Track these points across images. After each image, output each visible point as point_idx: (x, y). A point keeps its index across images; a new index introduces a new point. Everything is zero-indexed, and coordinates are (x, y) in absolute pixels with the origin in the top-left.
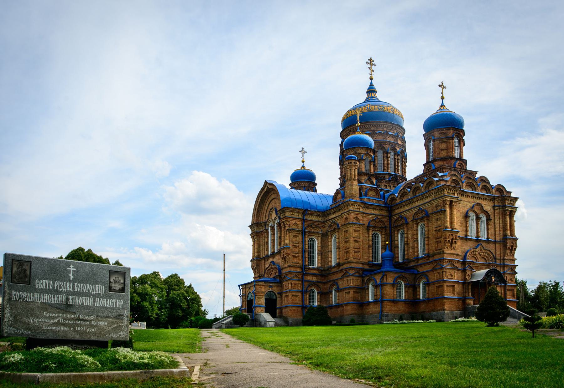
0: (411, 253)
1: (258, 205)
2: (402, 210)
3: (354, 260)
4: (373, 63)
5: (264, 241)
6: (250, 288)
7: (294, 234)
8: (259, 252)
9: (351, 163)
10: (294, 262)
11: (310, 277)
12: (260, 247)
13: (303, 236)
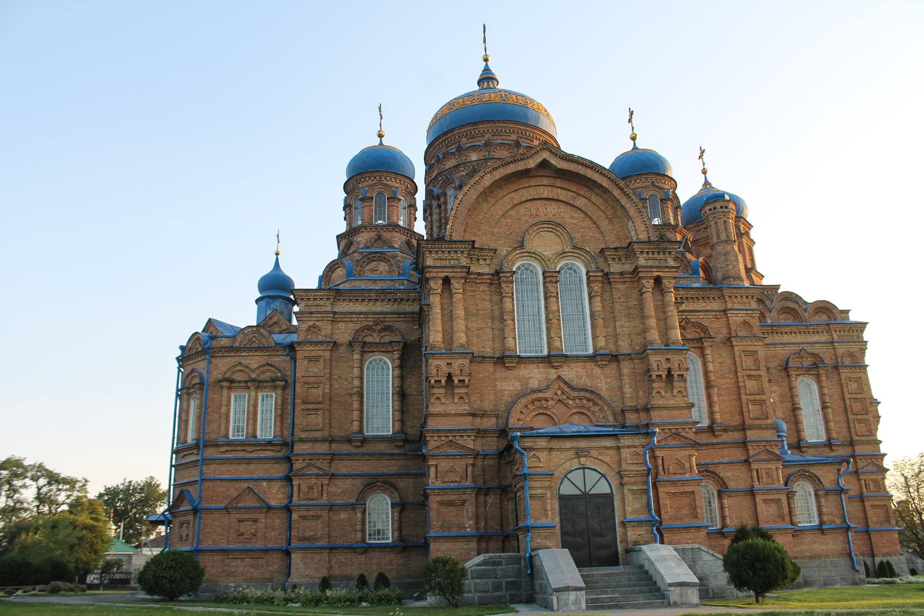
9: (726, 207)
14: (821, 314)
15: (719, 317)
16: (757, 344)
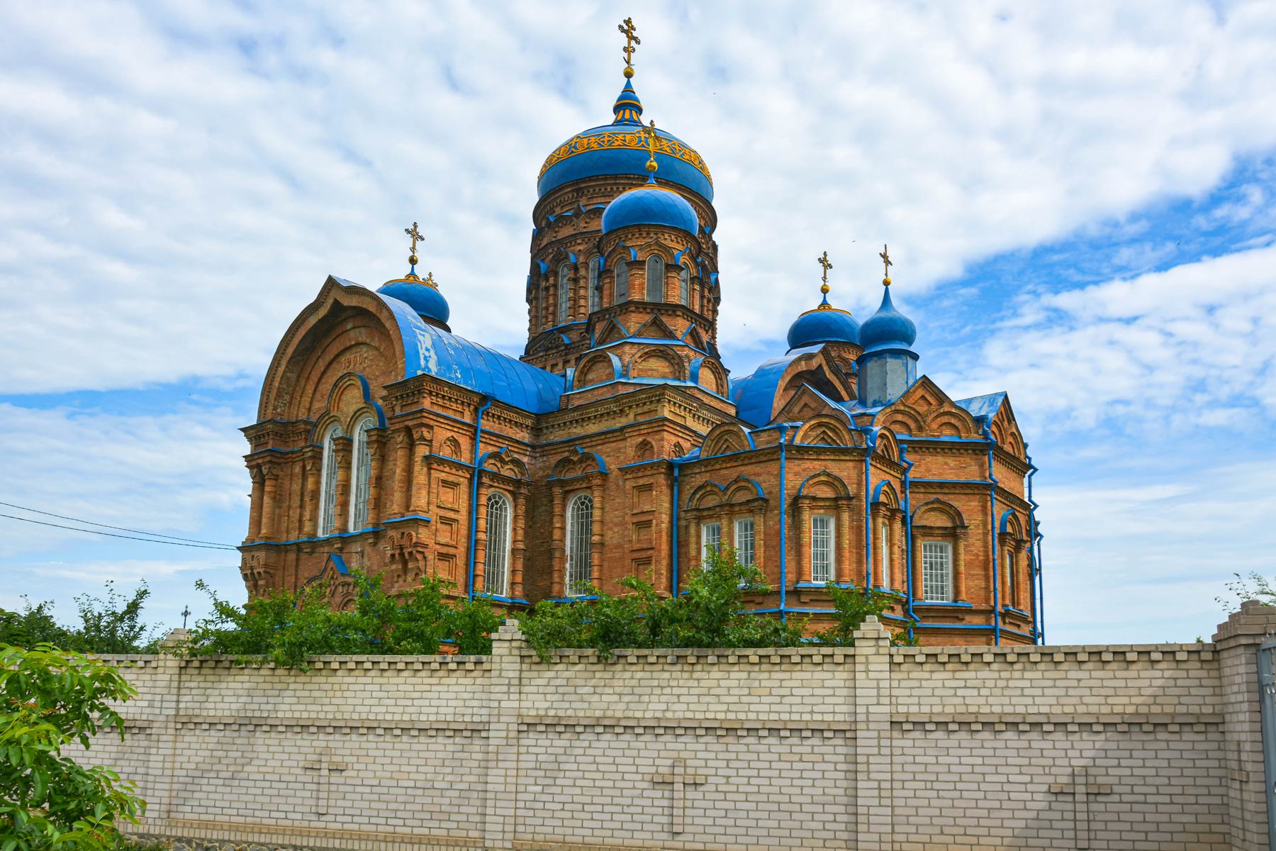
4: (635, 34)
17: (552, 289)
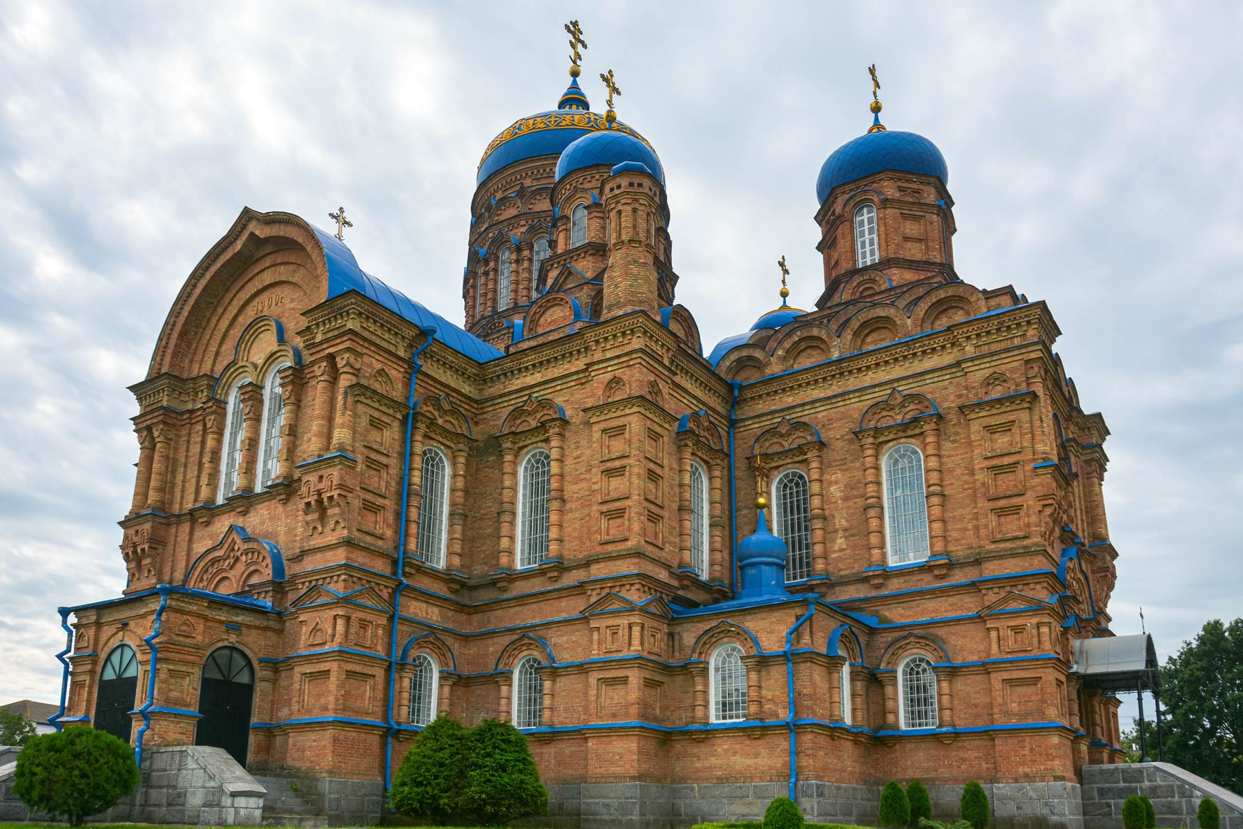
0: (841, 550)
1: (187, 308)
2: (790, 400)
3: (646, 546)
4: (581, 37)
5: (195, 449)
6: (125, 625)
7: (376, 414)
8: (166, 488)
10: (364, 528)
11: (415, 603)
12: (174, 472)
13: (404, 433)
14: (952, 311)
15: (584, 380)
16: (628, 411)
17: (492, 274)
